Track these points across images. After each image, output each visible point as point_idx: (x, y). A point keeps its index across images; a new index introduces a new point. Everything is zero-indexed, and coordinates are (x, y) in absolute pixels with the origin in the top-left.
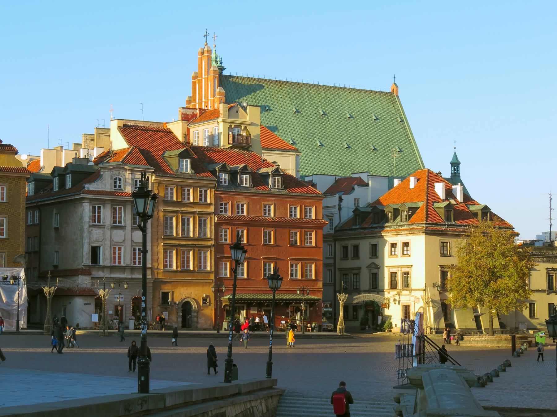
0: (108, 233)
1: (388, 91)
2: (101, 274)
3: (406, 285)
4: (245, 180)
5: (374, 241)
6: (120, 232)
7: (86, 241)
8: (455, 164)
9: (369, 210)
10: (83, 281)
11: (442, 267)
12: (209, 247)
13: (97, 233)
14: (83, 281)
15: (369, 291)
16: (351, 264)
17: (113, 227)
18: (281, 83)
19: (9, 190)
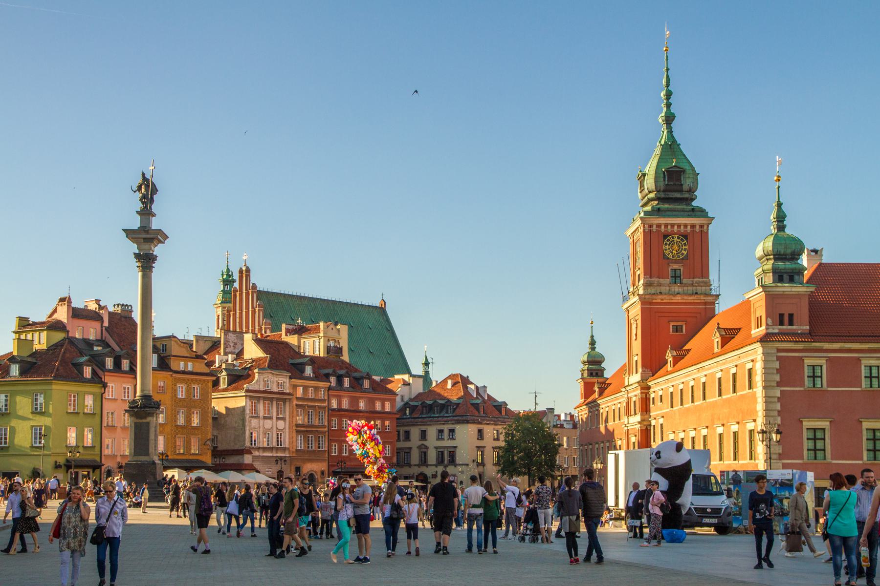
0: (261, 422)
1: (378, 305)
2: (256, 453)
3: (452, 461)
4: (346, 382)
5: (423, 428)
6: (269, 421)
7: (247, 428)
8: (427, 364)
9: (416, 404)
10: (247, 459)
11: (478, 448)
12: (324, 432)
13: (254, 422)
14: (247, 459)
15: (419, 466)
16: (402, 444)
17: (265, 418)
18: (301, 297)
19: (202, 389)
